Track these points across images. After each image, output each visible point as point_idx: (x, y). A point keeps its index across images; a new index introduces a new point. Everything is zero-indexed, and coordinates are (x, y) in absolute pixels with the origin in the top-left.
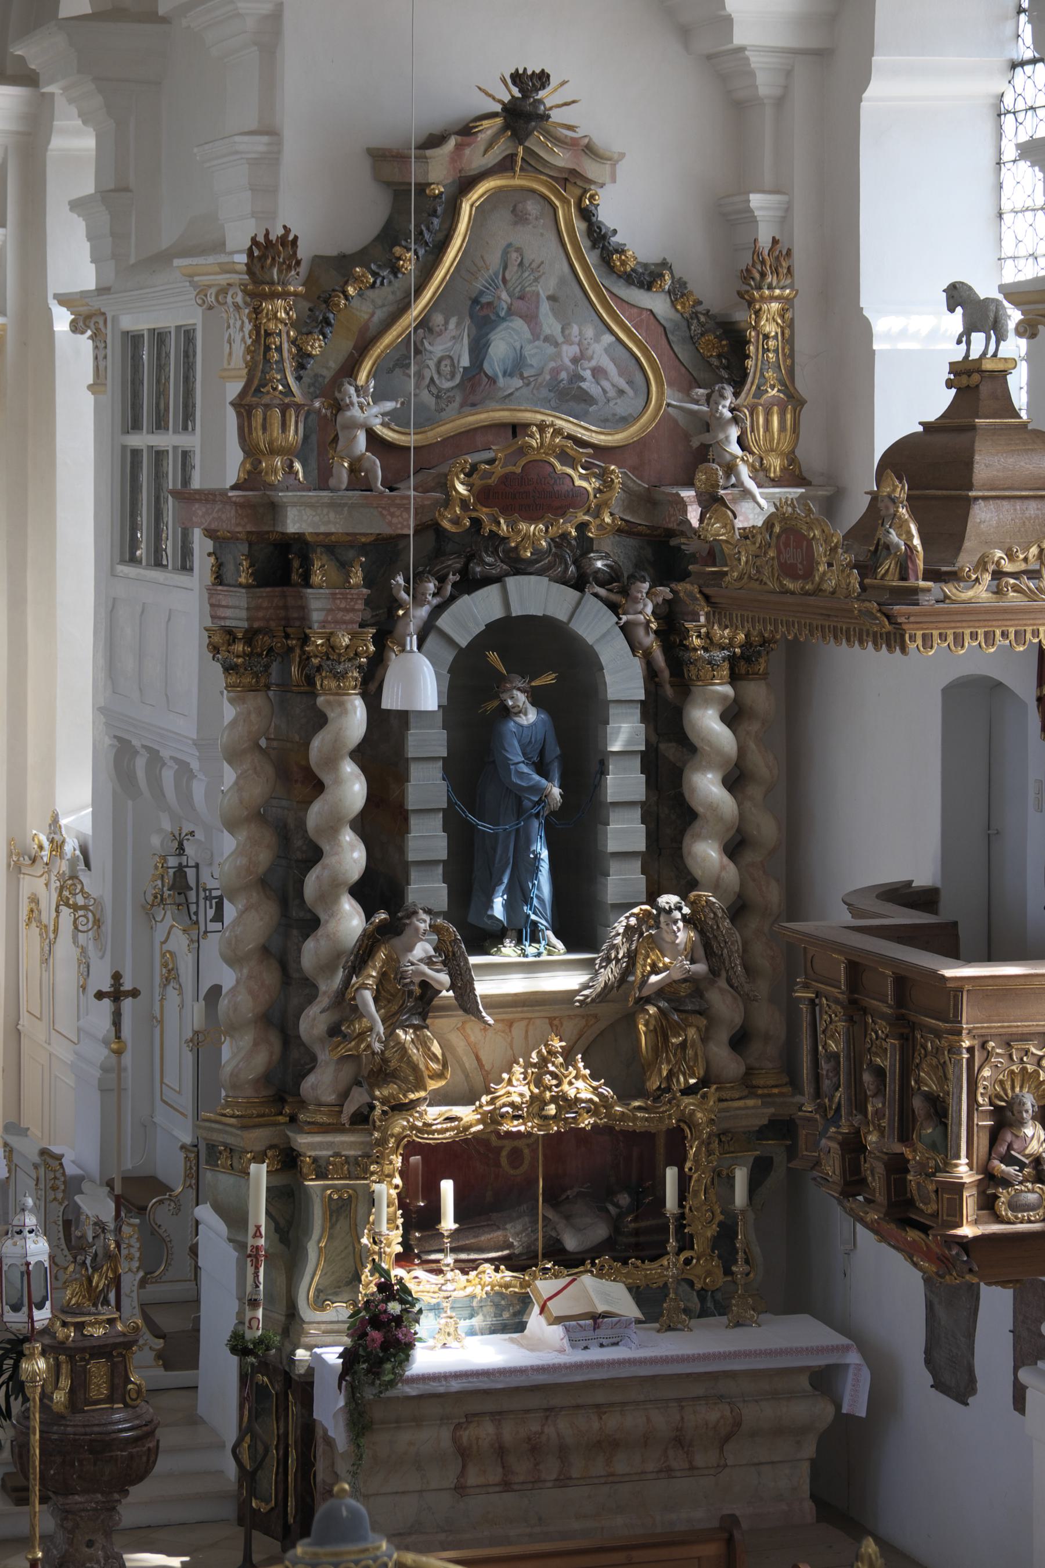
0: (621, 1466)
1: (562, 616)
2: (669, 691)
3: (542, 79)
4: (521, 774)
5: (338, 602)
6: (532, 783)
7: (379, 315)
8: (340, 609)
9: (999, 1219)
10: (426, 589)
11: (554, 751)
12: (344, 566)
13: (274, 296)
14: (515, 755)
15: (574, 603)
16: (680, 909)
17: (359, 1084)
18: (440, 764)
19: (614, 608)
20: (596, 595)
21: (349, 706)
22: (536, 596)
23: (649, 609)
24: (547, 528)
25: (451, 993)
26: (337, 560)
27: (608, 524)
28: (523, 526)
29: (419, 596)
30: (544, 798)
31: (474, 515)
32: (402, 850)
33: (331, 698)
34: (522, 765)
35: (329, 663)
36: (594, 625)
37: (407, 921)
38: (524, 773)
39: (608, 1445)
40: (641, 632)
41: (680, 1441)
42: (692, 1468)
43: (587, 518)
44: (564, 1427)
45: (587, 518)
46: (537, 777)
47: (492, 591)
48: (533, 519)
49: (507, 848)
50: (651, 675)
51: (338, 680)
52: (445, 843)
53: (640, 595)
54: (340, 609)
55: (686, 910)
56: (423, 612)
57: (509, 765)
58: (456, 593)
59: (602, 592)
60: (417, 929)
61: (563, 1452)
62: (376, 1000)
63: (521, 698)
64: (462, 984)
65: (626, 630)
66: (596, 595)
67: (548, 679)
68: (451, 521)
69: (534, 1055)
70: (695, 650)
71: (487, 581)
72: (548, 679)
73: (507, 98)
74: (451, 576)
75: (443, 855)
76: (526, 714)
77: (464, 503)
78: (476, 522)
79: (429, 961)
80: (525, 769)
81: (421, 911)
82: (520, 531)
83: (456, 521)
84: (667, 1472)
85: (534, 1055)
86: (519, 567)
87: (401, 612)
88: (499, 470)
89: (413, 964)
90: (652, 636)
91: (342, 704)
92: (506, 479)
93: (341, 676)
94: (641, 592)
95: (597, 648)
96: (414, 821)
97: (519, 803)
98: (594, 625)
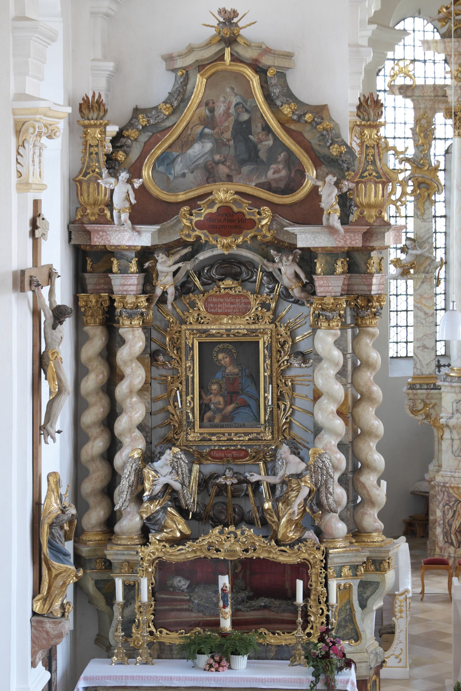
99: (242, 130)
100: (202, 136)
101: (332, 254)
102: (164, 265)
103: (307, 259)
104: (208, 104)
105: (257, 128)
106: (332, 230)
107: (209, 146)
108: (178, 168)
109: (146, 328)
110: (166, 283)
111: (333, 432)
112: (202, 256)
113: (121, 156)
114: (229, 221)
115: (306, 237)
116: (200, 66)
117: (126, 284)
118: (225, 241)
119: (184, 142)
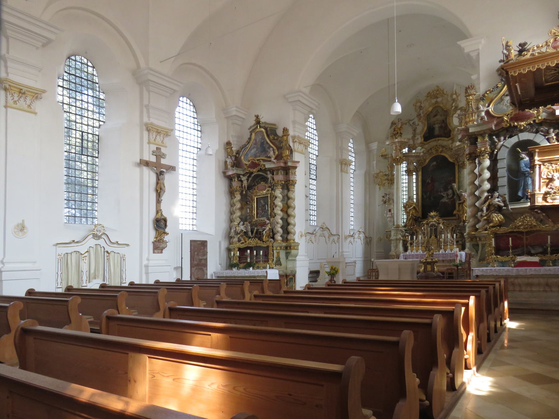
0: (534, 289)
1: (532, 139)
3: (525, 44)
7: (495, 96)
9: (547, 202)
12: (484, 138)
13: (469, 95)
22: (525, 136)
32: (497, 184)
39: (531, 285)
41: (547, 285)
42: (551, 291)
44: (519, 281)
48: (523, 121)
56: (502, 143)
61: (520, 285)
73: (518, 49)
77: (507, 121)
78: (510, 125)
83: (506, 125)
84: (546, 291)
86: (522, 131)
88: (513, 113)
92: (515, 115)
93: (483, 156)
96: (499, 179)
99: (262, 144)
100: (254, 147)
101: (278, 169)
102: (244, 179)
103: (272, 171)
104: (255, 140)
105: (265, 143)
106: (274, 163)
107: (255, 149)
108: (249, 156)
109: (241, 194)
110: (245, 183)
111: (279, 215)
112: (253, 175)
113: (237, 156)
114: (254, 165)
115: (268, 166)
116: (253, 130)
117: (236, 184)
118: (255, 170)
119: (250, 149)
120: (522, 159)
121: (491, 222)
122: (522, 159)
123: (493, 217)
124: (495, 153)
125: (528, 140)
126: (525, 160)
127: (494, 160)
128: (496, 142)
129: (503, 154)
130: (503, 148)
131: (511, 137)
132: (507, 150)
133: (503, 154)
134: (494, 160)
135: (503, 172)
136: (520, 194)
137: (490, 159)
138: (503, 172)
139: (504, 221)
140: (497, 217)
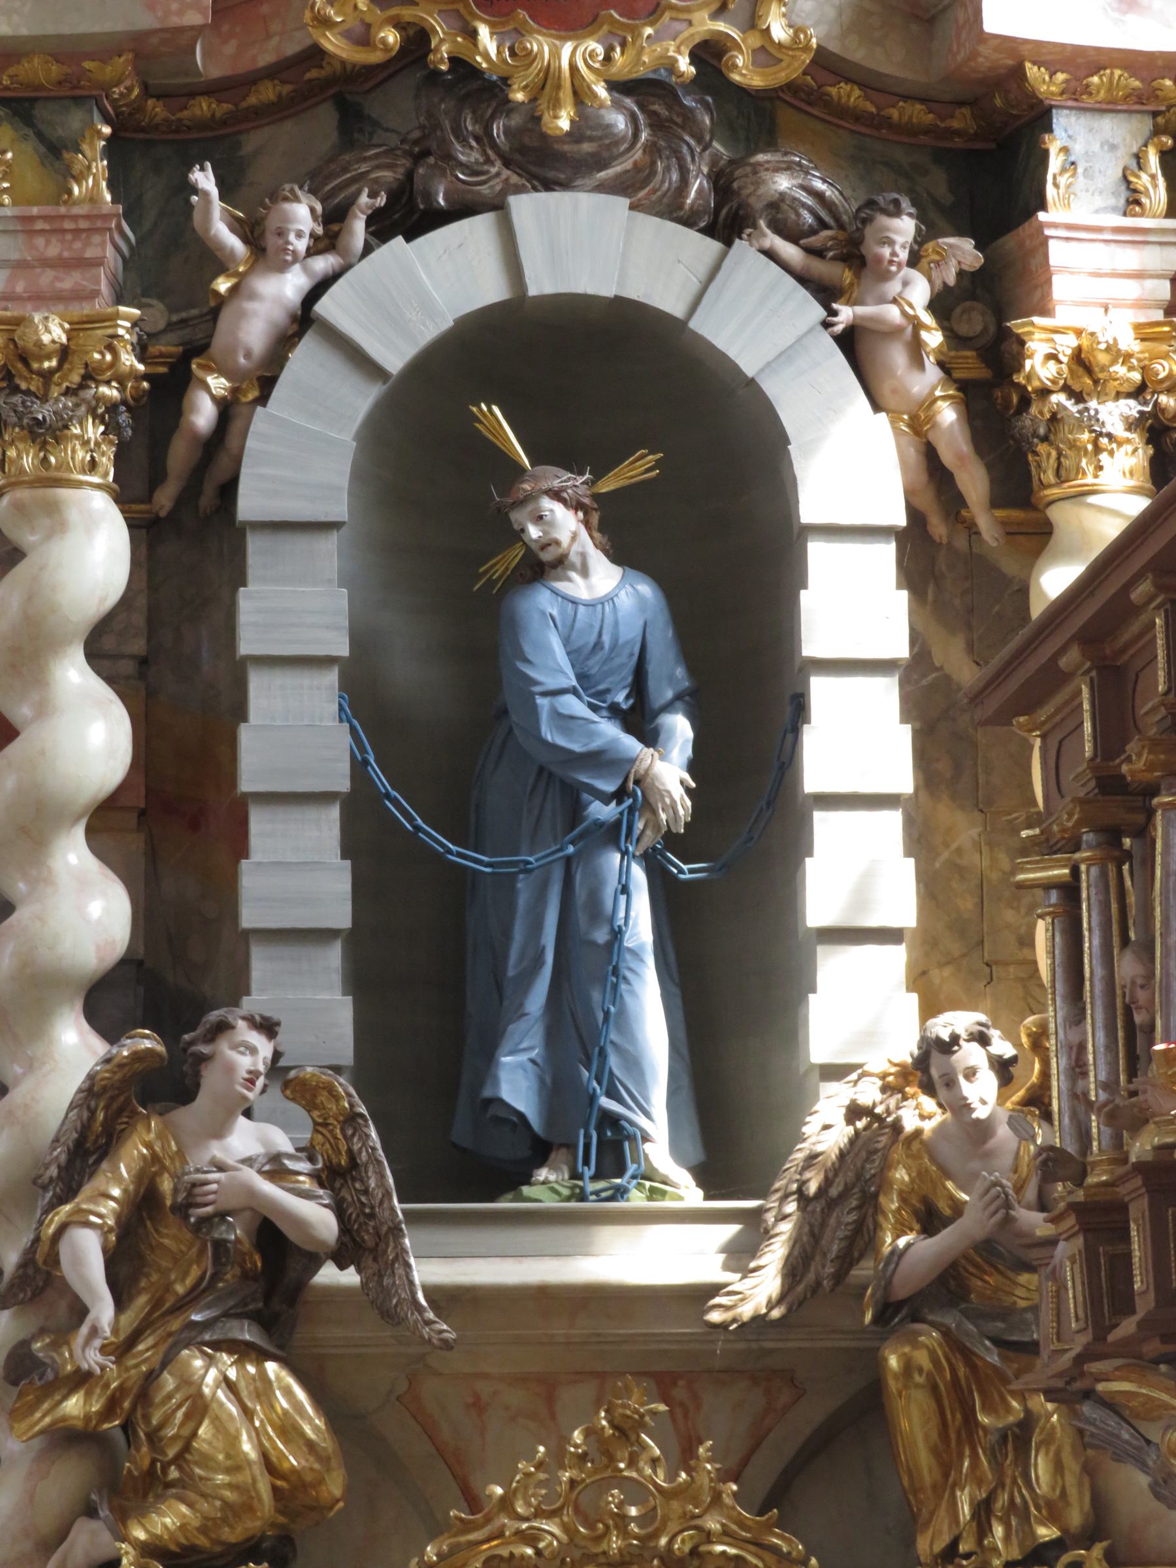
1: (672, 303)
2: (986, 522)
4: (565, 721)
5: (40, 241)
6: (595, 745)
8: (46, 263)
10: (287, 219)
11: (669, 675)
14: (550, 662)
15: (702, 270)
16: (983, 1040)
17: (91, 1512)
18: (332, 677)
19: (827, 294)
20: (770, 254)
21: (73, 515)
22: (593, 246)
23: (919, 292)
24: (609, 50)
25: (350, 1277)
26: (40, 136)
27: (780, 45)
28: (540, 44)
29: (271, 241)
30: (635, 792)
31: (408, 13)
33: (23, 494)
34: (570, 699)
35: (17, 399)
36: (756, 318)
37: (205, 1049)
38: (576, 722)
40: (898, 357)
43: (721, 26)
45: (721, 26)
46: (610, 731)
47: (476, 232)
49: (536, 927)
50: (932, 473)
51: (43, 446)
52: (344, 885)
53: (886, 251)
54: (46, 263)
55: (1003, 1048)
56: (291, 285)
57: (533, 694)
58: (373, 241)
59: (790, 251)
60: (230, 1069)
62: (113, 1261)
63: (565, 524)
64: (365, 1241)
65: (852, 343)
66: (770, 254)
67: (638, 468)
68: (347, 35)
69: (577, 1436)
70: (1045, 392)
71: (461, 210)
72: (638, 468)
74: (364, 199)
75: (341, 916)
76: (585, 572)
79: (276, 1169)
80: (575, 706)
81: (241, 1024)
82: (530, 57)
85: (577, 1436)
86: (546, 164)
87: (223, 285)
89: (221, 1168)
90: (932, 373)
91: (53, 509)
93: (45, 434)
94: (891, 243)
95: (771, 388)
96: (260, 823)
97: (563, 799)
98: (756, 318)
120: (541, 566)
121: (151, 1487)
122: (541, 566)
123: (199, 1408)
124: (203, 414)
125: (620, 304)
126: (577, 587)
127: (190, 523)
128: (218, 262)
129: (302, 457)
130: (307, 361)
131: (406, 217)
132: (361, 399)
133: (302, 457)
134: (190, 523)
135: (293, 733)
136: (516, 1083)
137: (124, 495)
138: (293, 733)
139: (335, 1486)
140: (249, 1411)
